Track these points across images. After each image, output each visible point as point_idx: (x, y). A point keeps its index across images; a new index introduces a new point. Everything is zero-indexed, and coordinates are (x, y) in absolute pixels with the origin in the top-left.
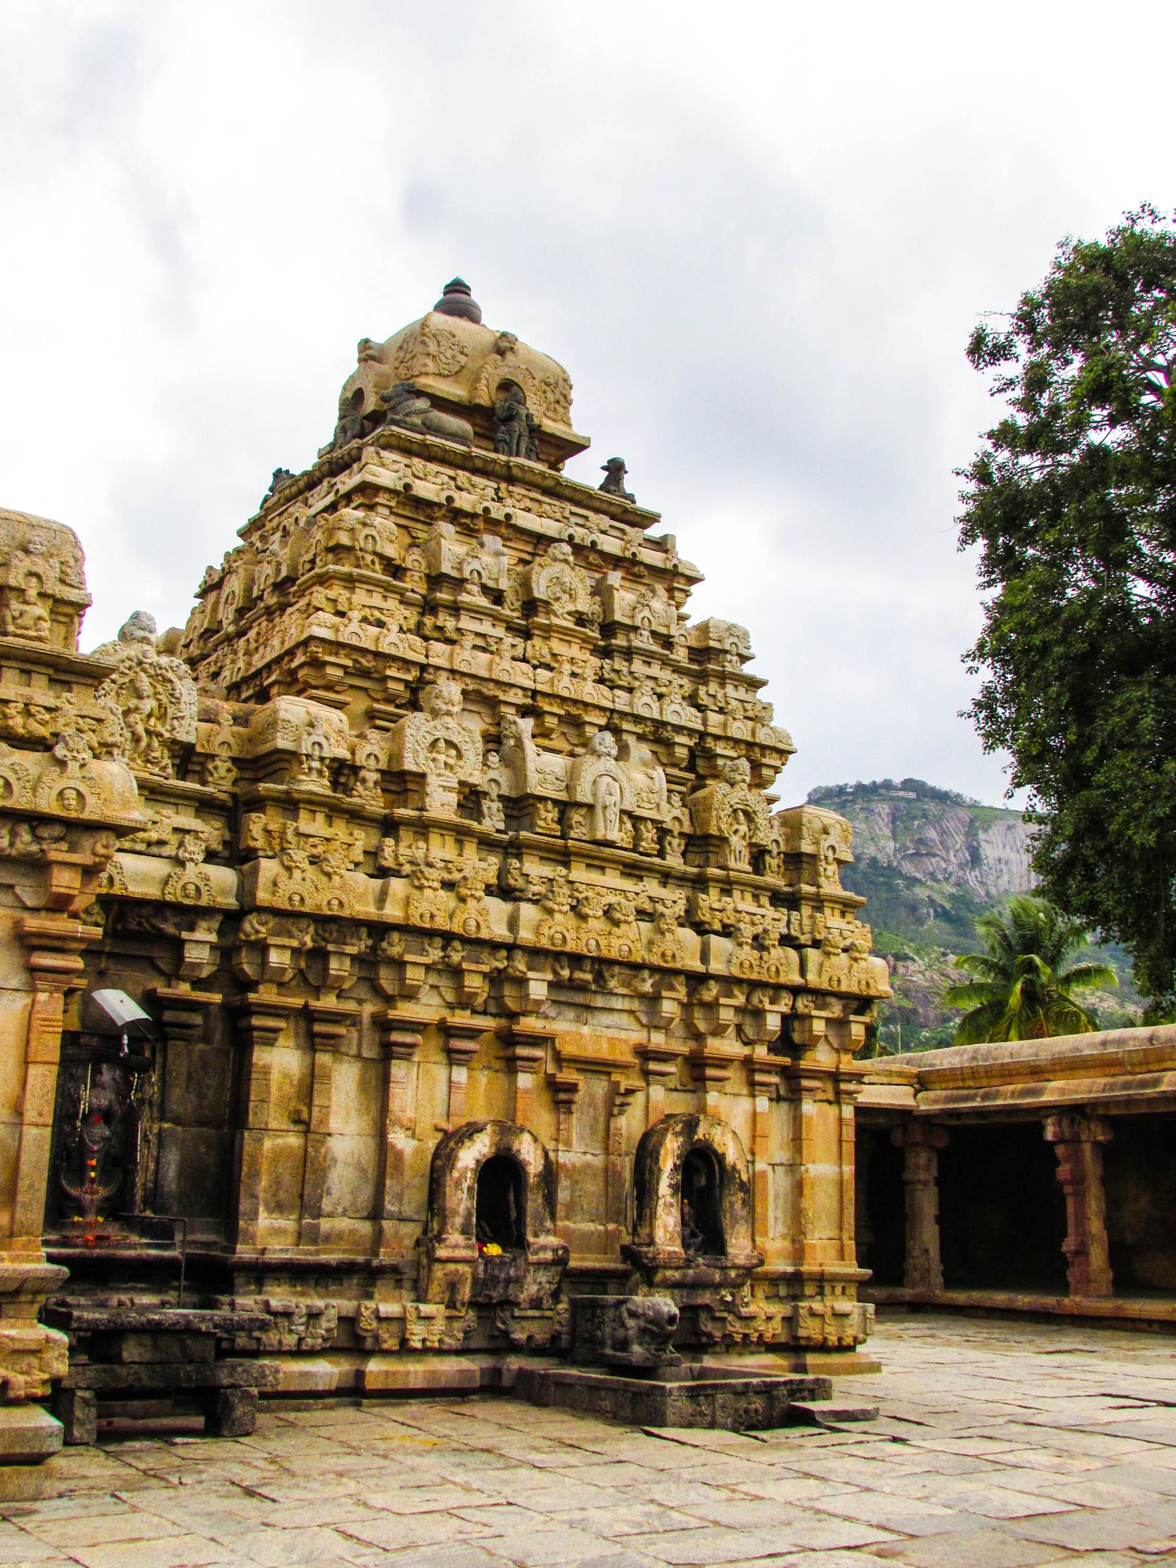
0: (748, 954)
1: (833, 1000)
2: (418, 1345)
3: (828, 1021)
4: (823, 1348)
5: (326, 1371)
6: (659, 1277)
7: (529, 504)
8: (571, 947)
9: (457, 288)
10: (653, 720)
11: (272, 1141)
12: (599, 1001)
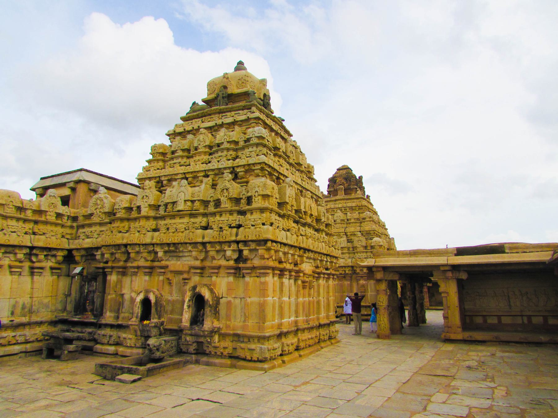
0: (216, 234)
1: (250, 243)
2: (128, 345)
3: (251, 250)
4: (245, 359)
5: (112, 349)
6: (184, 332)
7: (209, 120)
8: (165, 242)
9: (240, 63)
10: (217, 169)
11: (110, 296)
12: (181, 254)
